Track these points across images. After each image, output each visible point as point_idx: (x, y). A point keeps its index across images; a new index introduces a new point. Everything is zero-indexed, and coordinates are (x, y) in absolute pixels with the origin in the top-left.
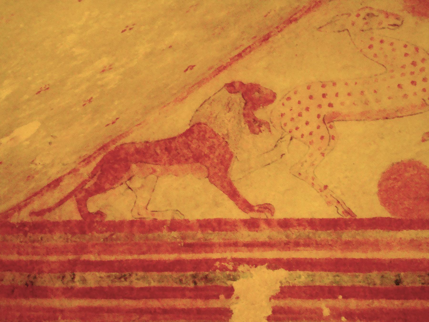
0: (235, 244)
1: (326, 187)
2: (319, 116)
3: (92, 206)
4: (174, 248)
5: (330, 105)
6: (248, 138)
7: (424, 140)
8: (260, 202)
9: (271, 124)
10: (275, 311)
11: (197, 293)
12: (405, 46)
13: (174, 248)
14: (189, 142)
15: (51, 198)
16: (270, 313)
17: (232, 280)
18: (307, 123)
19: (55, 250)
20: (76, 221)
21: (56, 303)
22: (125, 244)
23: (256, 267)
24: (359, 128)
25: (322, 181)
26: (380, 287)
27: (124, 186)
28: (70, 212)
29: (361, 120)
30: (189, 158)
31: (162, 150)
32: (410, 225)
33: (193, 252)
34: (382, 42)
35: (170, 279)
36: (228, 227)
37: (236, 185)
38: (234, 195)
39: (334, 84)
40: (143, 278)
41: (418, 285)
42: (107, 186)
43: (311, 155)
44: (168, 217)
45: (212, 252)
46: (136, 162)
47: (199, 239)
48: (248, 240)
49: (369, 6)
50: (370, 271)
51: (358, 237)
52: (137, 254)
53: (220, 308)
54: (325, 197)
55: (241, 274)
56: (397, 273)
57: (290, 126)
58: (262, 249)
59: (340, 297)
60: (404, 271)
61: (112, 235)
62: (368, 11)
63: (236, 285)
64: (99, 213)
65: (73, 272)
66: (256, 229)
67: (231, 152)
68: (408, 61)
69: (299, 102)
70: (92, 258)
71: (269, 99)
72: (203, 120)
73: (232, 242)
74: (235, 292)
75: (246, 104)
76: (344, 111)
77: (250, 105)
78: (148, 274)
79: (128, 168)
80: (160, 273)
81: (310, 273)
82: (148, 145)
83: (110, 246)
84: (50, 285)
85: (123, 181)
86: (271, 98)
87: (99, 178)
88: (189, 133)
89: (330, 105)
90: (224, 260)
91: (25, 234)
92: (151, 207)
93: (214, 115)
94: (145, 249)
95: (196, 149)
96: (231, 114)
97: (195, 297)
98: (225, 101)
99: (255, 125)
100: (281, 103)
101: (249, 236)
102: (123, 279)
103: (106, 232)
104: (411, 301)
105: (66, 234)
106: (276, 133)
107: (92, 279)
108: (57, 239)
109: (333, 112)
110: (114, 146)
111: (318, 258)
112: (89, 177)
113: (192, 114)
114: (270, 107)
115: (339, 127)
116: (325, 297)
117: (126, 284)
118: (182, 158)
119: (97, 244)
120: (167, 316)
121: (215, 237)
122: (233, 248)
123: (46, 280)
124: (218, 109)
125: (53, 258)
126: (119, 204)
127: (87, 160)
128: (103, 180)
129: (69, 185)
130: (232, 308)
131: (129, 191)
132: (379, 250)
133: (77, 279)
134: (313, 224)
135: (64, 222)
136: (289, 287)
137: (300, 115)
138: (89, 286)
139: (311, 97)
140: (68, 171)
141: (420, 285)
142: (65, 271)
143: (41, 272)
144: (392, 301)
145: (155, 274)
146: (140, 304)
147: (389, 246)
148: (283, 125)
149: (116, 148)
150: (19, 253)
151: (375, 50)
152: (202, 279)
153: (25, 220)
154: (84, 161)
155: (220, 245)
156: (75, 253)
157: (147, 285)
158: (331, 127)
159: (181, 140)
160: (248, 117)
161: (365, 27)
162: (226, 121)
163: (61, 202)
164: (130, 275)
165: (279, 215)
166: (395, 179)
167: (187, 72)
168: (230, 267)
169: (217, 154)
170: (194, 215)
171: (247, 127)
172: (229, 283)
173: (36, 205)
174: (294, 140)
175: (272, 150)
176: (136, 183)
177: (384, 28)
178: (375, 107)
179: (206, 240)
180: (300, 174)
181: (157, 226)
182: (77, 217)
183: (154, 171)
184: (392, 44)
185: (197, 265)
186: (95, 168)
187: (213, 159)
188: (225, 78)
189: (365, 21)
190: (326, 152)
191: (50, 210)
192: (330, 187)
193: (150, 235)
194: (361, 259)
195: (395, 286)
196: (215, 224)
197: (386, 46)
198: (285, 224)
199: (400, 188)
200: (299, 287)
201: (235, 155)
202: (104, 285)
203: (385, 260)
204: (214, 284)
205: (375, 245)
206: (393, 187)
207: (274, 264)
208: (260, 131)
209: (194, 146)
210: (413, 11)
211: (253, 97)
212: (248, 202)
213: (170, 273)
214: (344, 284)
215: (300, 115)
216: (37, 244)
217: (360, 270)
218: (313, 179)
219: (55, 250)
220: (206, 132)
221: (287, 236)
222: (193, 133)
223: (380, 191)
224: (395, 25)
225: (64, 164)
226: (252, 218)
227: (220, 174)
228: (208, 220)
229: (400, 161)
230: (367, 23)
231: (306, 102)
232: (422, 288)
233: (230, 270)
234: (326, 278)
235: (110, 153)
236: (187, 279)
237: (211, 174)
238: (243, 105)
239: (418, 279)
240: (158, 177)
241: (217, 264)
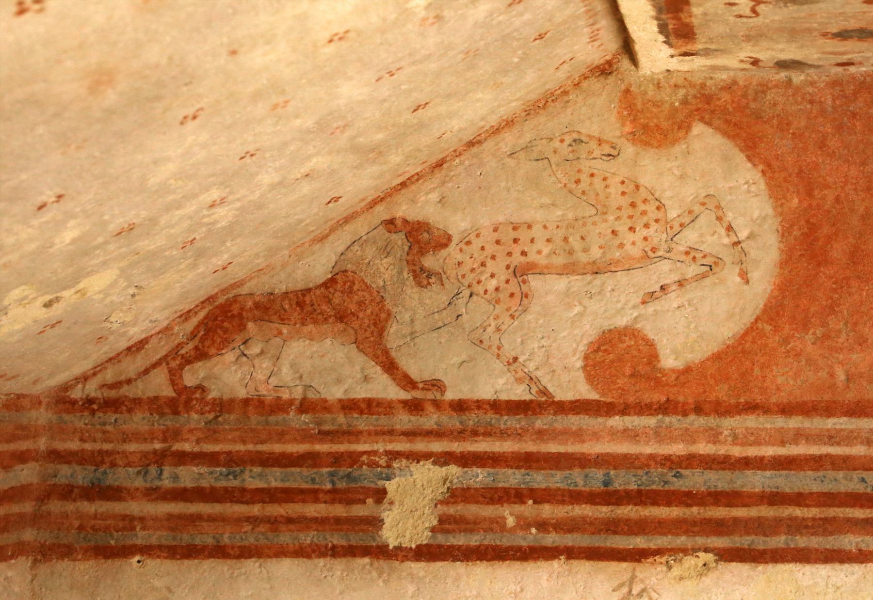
0: (391, 432)
1: (515, 359)
2: (508, 267)
3: (190, 379)
4: (305, 436)
5: (524, 253)
6: (412, 292)
7: (644, 303)
8: (427, 377)
9: (444, 277)
10: (443, 520)
11: (336, 496)
12: (623, 183)
13: (305, 436)
14: (331, 296)
15: (132, 366)
16: (435, 522)
17: (383, 479)
18: (492, 276)
19: (137, 437)
20: (166, 397)
21: (134, 507)
22: (236, 430)
23: (418, 462)
24: (561, 284)
25: (509, 351)
26: (583, 489)
27: (237, 351)
28: (159, 384)
29: (562, 274)
30: (330, 317)
31: (291, 305)
32: (625, 411)
33: (332, 442)
34: (592, 175)
35: (298, 478)
36: (380, 410)
37: (393, 354)
38: (390, 367)
39: (529, 227)
40: (260, 475)
41: (633, 487)
42: (213, 351)
43: (497, 318)
44: (298, 393)
45: (357, 441)
46: (255, 320)
47: (340, 425)
48: (408, 427)
49: (576, 129)
50: (570, 468)
51: (556, 425)
52: (253, 443)
53: (367, 516)
54: (513, 373)
55: (397, 472)
56: (606, 471)
57: (470, 278)
58: (426, 439)
59: (530, 502)
60: (615, 468)
61: (217, 417)
62: (575, 136)
63: (391, 486)
64: (201, 388)
65: (160, 465)
66: (420, 413)
67: (388, 310)
68: (624, 201)
69: (483, 248)
70: (187, 447)
71: (443, 242)
72: (349, 267)
73: (386, 428)
74: (389, 496)
75: (410, 247)
76: (542, 260)
77: (416, 249)
78: (268, 470)
79: (242, 327)
80: (283, 470)
81: (491, 470)
82: (272, 297)
83: (215, 432)
84: (127, 484)
85: (236, 344)
86: (444, 241)
87: (202, 340)
88: (331, 282)
89: (524, 253)
90: (375, 453)
91: (93, 413)
92: (273, 381)
93: (367, 261)
94: (263, 437)
95: (339, 304)
96: (389, 260)
97: (333, 502)
98: (381, 244)
99: (423, 277)
100: (458, 248)
101: (410, 421)
102: (231, 477)
103: (209, 412)
104: (623, 507)
105: (151, 414)
106: (451, 287)
107: (189, 476)
108: (139, 421)
109: (528, 263)
110: (225, 297)
111: (502, 451)
112: (188, 339)
113: (334, 258)
114: (444, 253)
115: (535, 282)
116: (509, 501)
117: (235, 483)
118: (320, 317)
119: (195, 429)
120: (292, 527)
121: (362, 423)
122: (387, 438)
123: (123, 476)
124: (370, 252)
125: (132, 447)
126: (229, 375)
127: (186, 316)
128: (207, 343)
129: (159, 349)
130: (384, 515)
131: (244, 359)
132: (583, 442)
133: (166, 474)
134: (496, 406)
135: (148, 398)
136: (463, 489)
137: (483, 264)
138: (182, 485)
139: (498, 242)
140: (157, 329)
141: (636, 487)
142: (148, 465)
143: (113, 465)
144: (599, 507)
145: (277, 471)
146: (256, 510)
147: (596, 436)
148: (460, 277)
149: (227, 300)
150: (82, 440)
151: (583, 186)
152: (342, 478)
153: (93, 395)
154: (181, 316)
155: (369, 433)
156: (165, 440)
157: (265, 485)
158: (524, 282)
159: (318, 292)
160: (414, 265)
161: (571, 157)
162: (382, 270)
163: (146, 371)
164: (242, 472)
165: (450, 395)
166: (606, 350)
167: (330, 205)
168: (383, 462)
169: (369, 312)
170: (336, 393)
171: (412, 278)
172: (381, 483)
173: (109, 376)
174: (475, 297)
175: (445, 309)
176: (255, 349)
177: (595, 159)
178: (583, 258)
179: (350, 426)
180: (481, 341)
181: (279, 406)
182: (168, 392)
183: (280, 333)
184: (605, 179)
185: (337, 459)
186: (197, 327)
187: (363, 319)
188: (382, 212)
189: (571, 148)
190: (517, 314)
191: (129, 381)
192: (521, 360)
193: (272, 419)
194: (559, 453)
195: (602, 488)
196: (363, 406)
197: (597, 181)
198: (460, 406)
199: (612, 362)
200: (476, 489)
201: (393, 314)
202: (205, 484)
203: (589, 455)
204: (359, 484)
205: (578, 435)
206: (603, 362)
207: (444, 459)
208: (429, 284)
209: (336, 301)
210: (633, 137)
211: (420, 241)
212: (410, 378)
213: (298, 470)
214: (536, 486)
215: (483, 264)
216: (109, 428)
217: (558, 468)
218: (499, 348)
219: (137, 437)
220: (353, 283)
221: (461, 423)
222: (336, 283)
223: (586, 366)
224: (610, 155)
225: (151, 321)
226: (415, 399)
227: (372, 339)
228: (353, 400)
229: (612, 327)
230: (573, 151)
231: (491, 249)
232: (639, 492)
233: (381, 466)
234: (512, 478)
235: (217, 307)
236: (323, 477)
237: (360, 338)
238: (406, 248)
239: (634, 479)
240: (285, 341)
241: (364, 458)
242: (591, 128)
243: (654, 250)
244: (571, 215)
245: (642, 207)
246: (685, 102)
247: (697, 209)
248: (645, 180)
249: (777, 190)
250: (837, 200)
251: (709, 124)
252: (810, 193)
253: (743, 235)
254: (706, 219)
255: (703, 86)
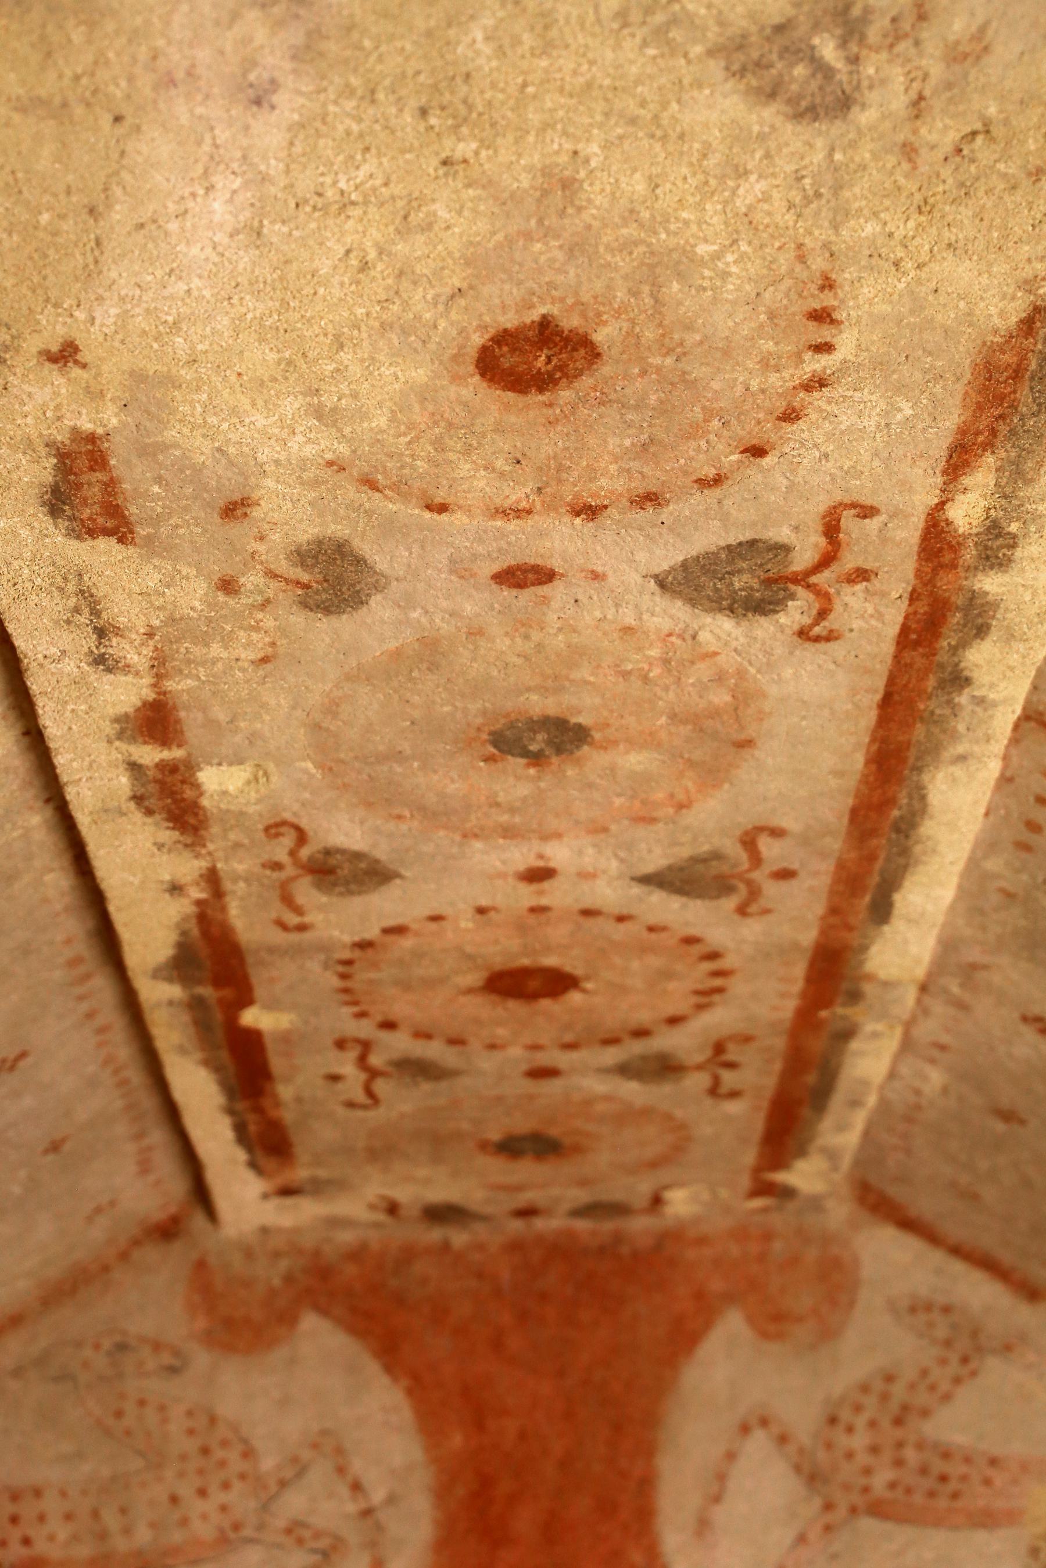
39: (38, 1493)
62: (118, 1338)
68: (191, 1445)
89: (26, 1541)
242: (143, 1325)
243: (236, 1527)
244: (106, 1472)
245: (219, 1454)
246: (289, 1279)
247: (306, 1454)
248: (227, 1408)
249: (430, 1422)
250: (522, 1436)
251: (324, 1312)
252: (480, 1426)
253: (378, 1496)
254: (319, 1473)
255: (317, 1253)
